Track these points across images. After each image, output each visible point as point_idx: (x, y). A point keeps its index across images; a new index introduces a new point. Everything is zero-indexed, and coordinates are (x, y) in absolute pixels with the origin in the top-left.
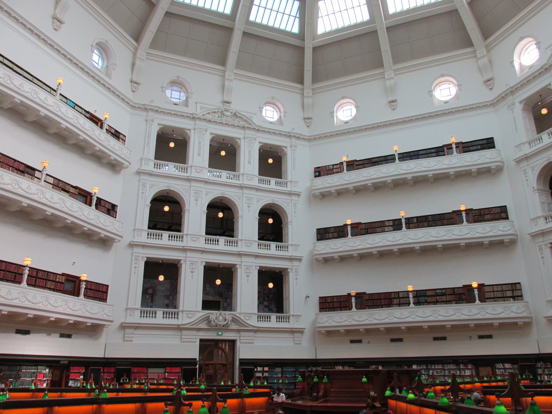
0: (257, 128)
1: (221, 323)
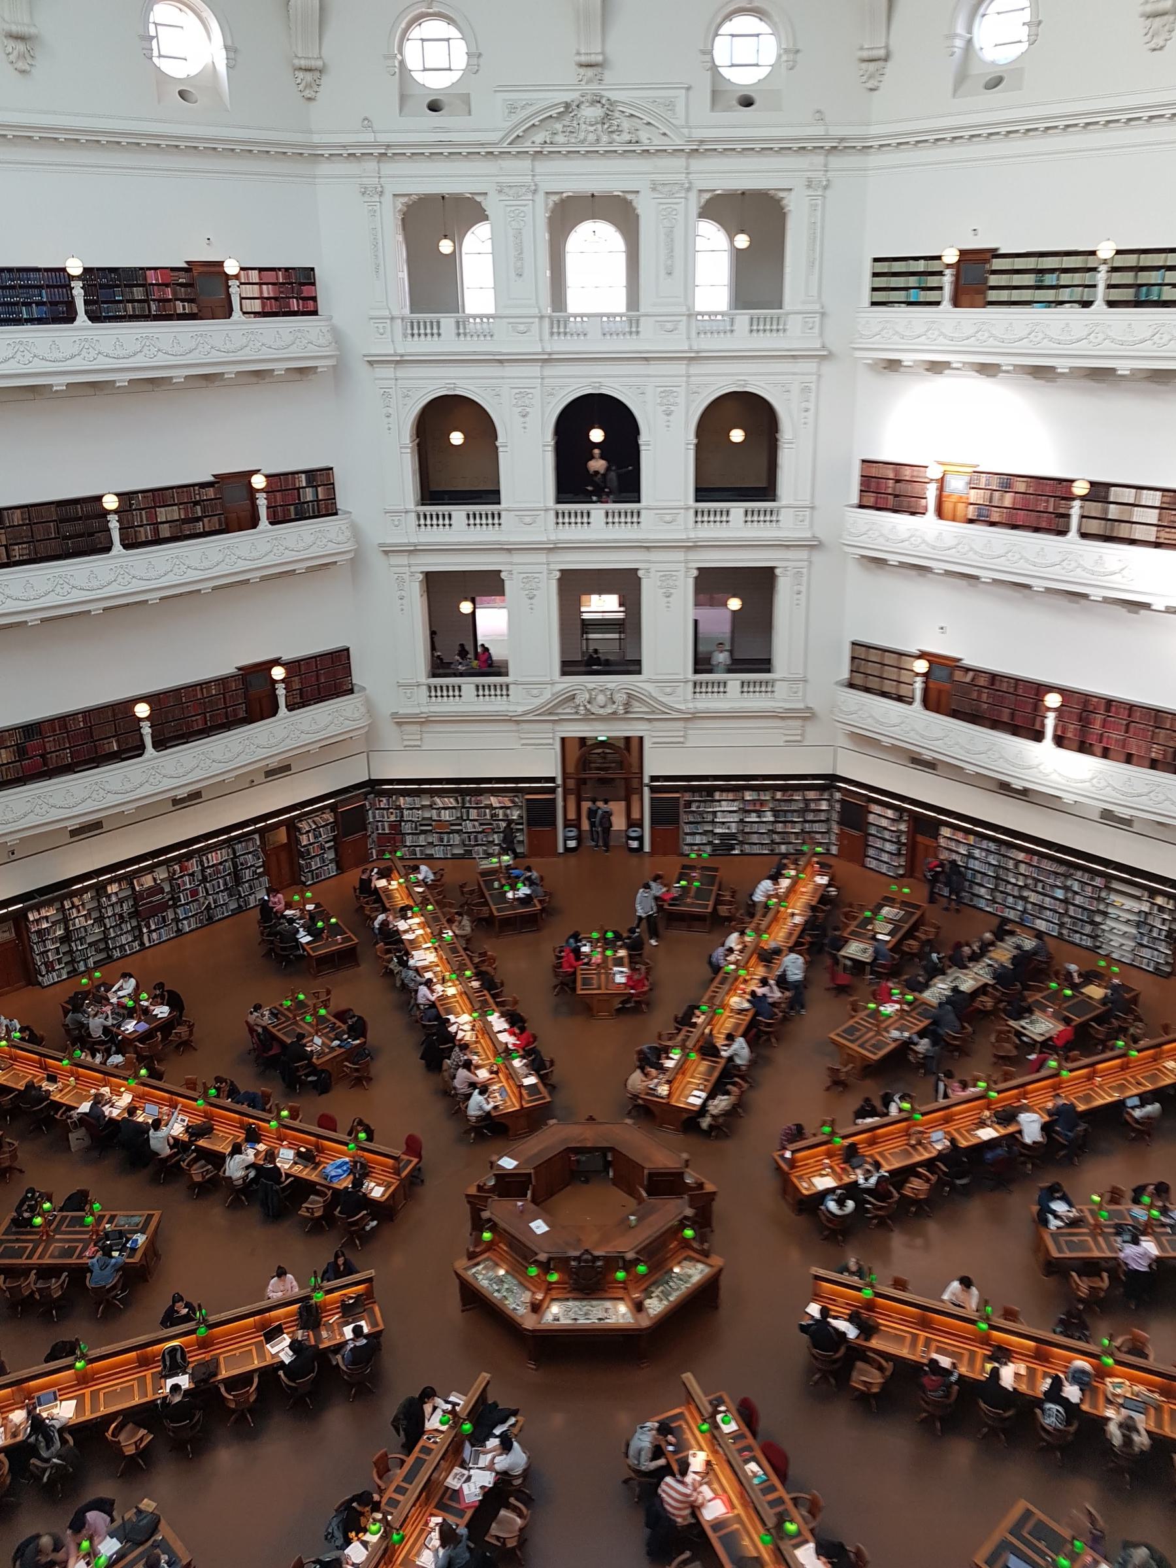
0: (688, 148)
1: (601, 711)
